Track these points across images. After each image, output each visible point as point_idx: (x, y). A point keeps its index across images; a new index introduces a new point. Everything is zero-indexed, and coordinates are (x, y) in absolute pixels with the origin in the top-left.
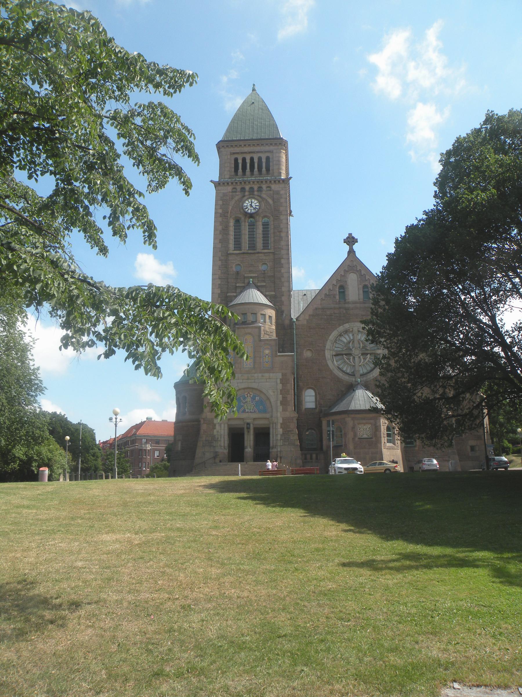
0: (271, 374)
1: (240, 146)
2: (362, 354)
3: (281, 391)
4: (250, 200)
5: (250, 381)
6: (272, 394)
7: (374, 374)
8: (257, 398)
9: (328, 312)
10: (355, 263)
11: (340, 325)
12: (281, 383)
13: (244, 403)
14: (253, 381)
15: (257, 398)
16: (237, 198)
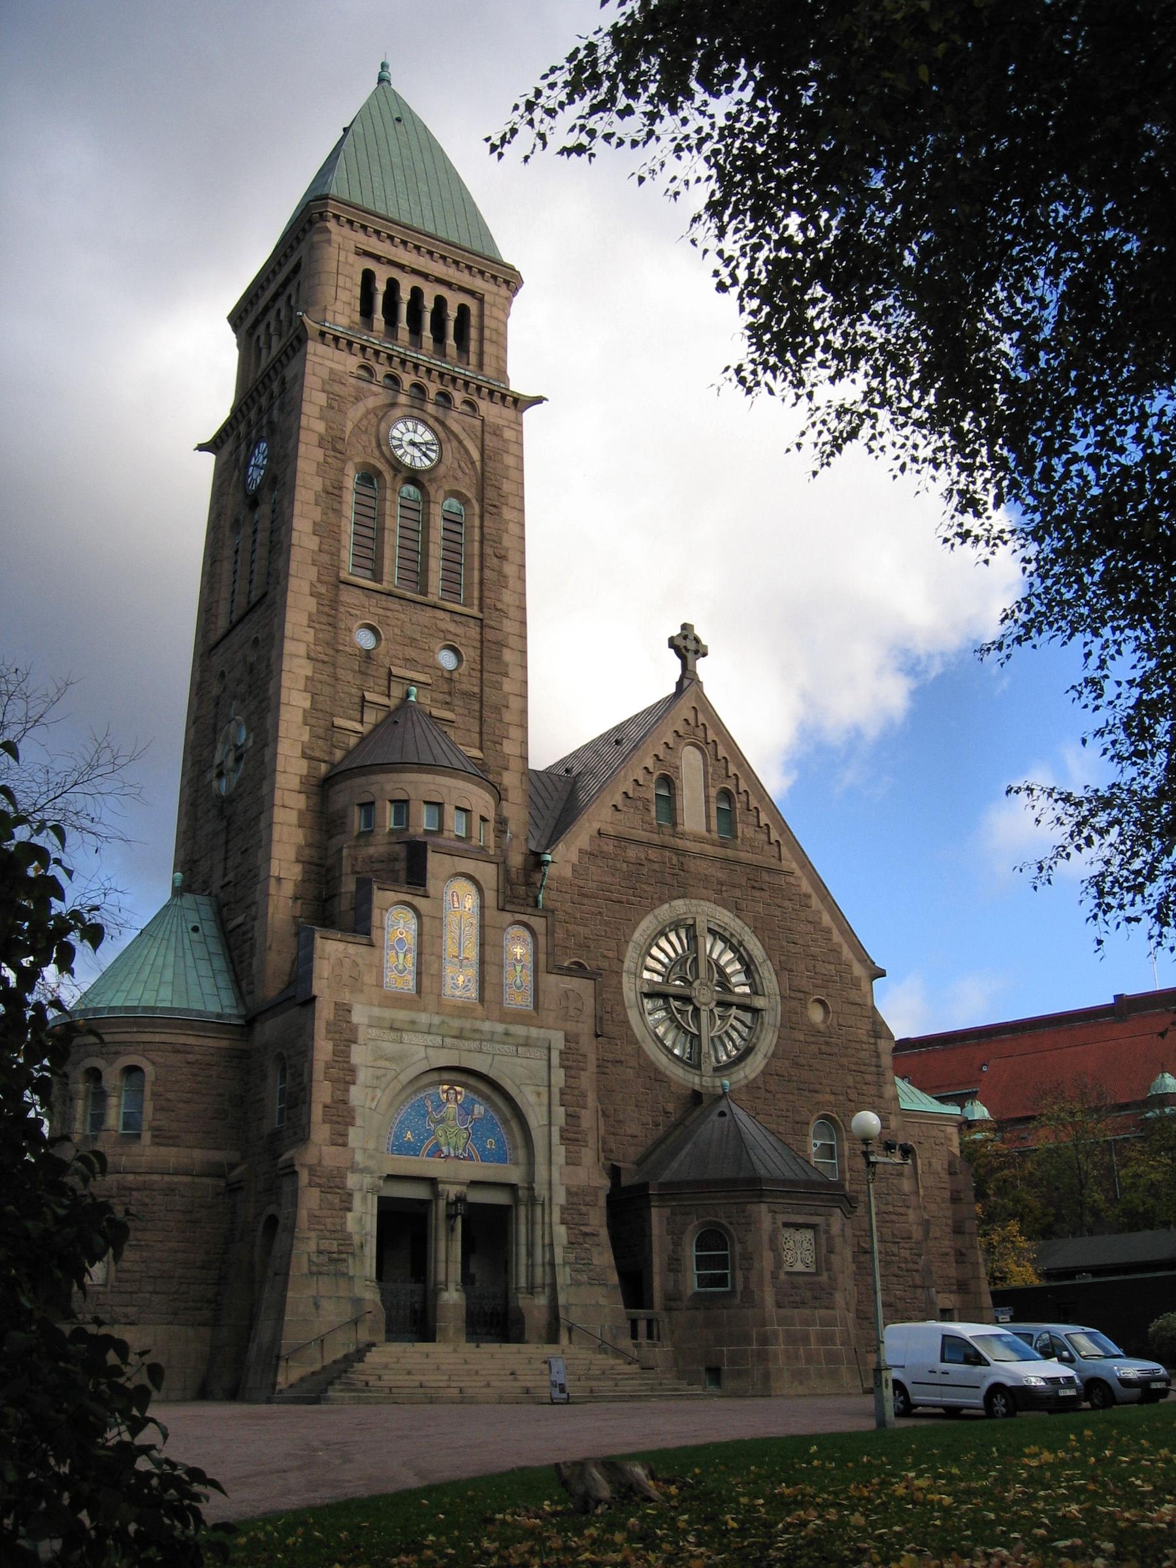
0: (534, 1032)
1: (391, 238)
2: (720, 1004)
3: (562, 1093)
4: (410, 425)
5: (466, 1044)
6: (532, 1098)
7: (747, 1070)
9: (633, 853)
10: (702, 719)
11: (662, 901)
12: (562, 1066)
16: (371, 402)
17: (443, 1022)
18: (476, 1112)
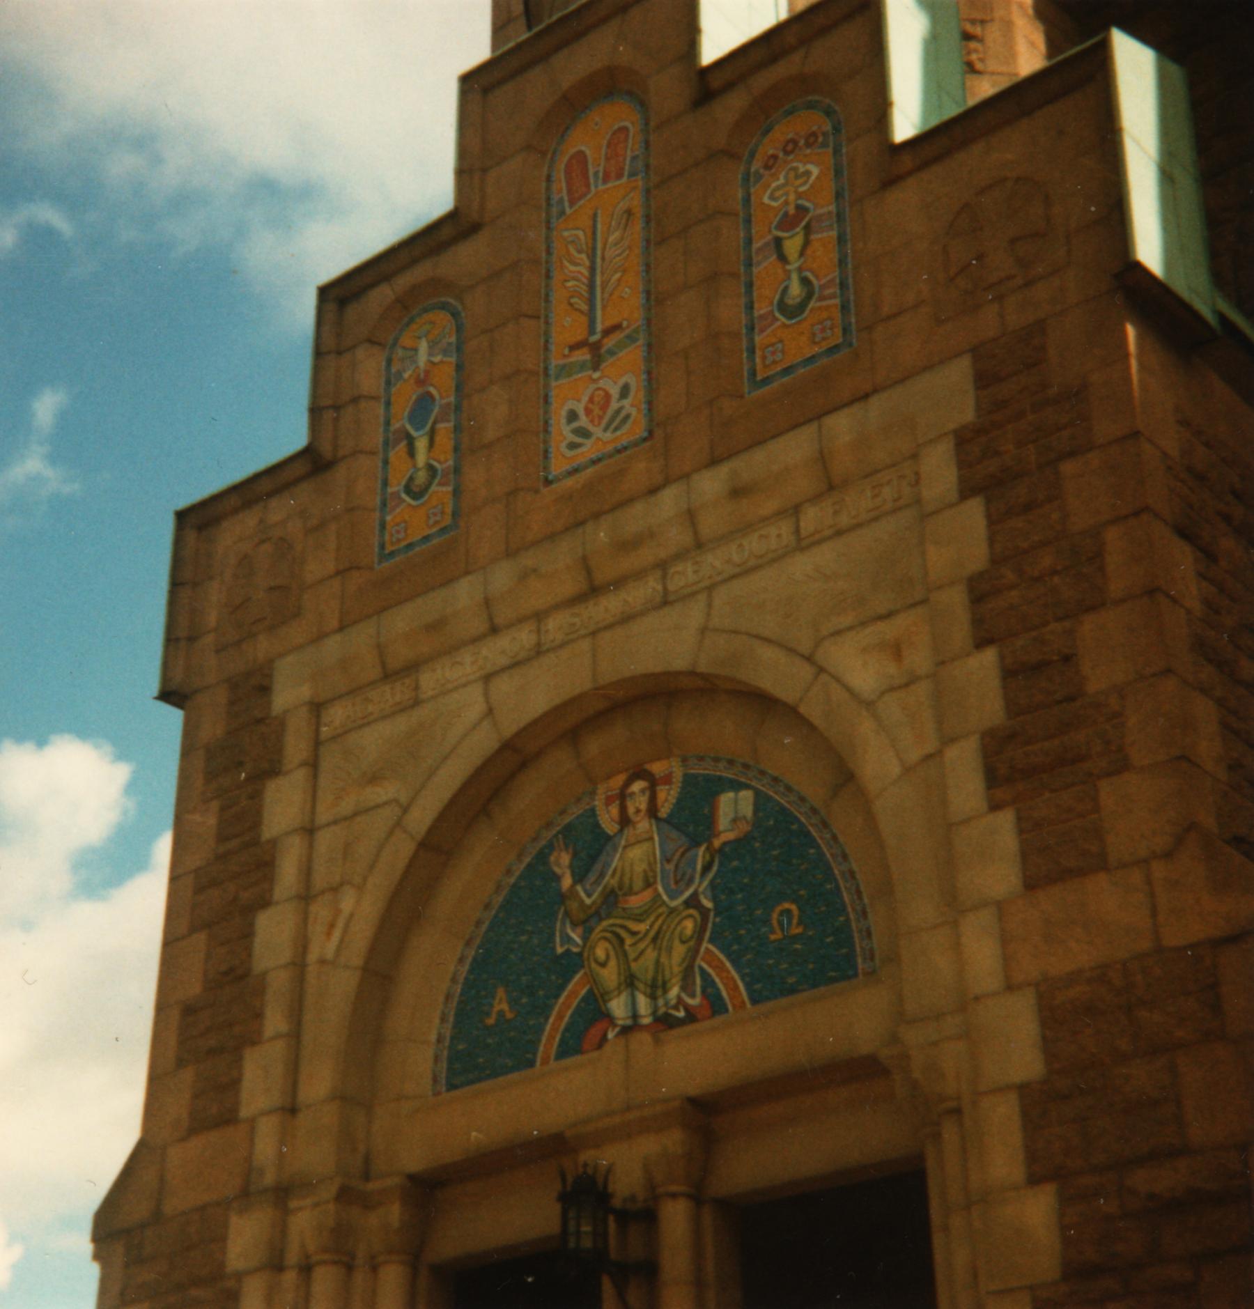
0: (842, 425)
3: (980, 591)
5: (610, 605)
8: (733, 810)
13: (586, 922)
14: (650, 587)
15: (733, 810)
17: (524, 576)
18: (723, 822)
